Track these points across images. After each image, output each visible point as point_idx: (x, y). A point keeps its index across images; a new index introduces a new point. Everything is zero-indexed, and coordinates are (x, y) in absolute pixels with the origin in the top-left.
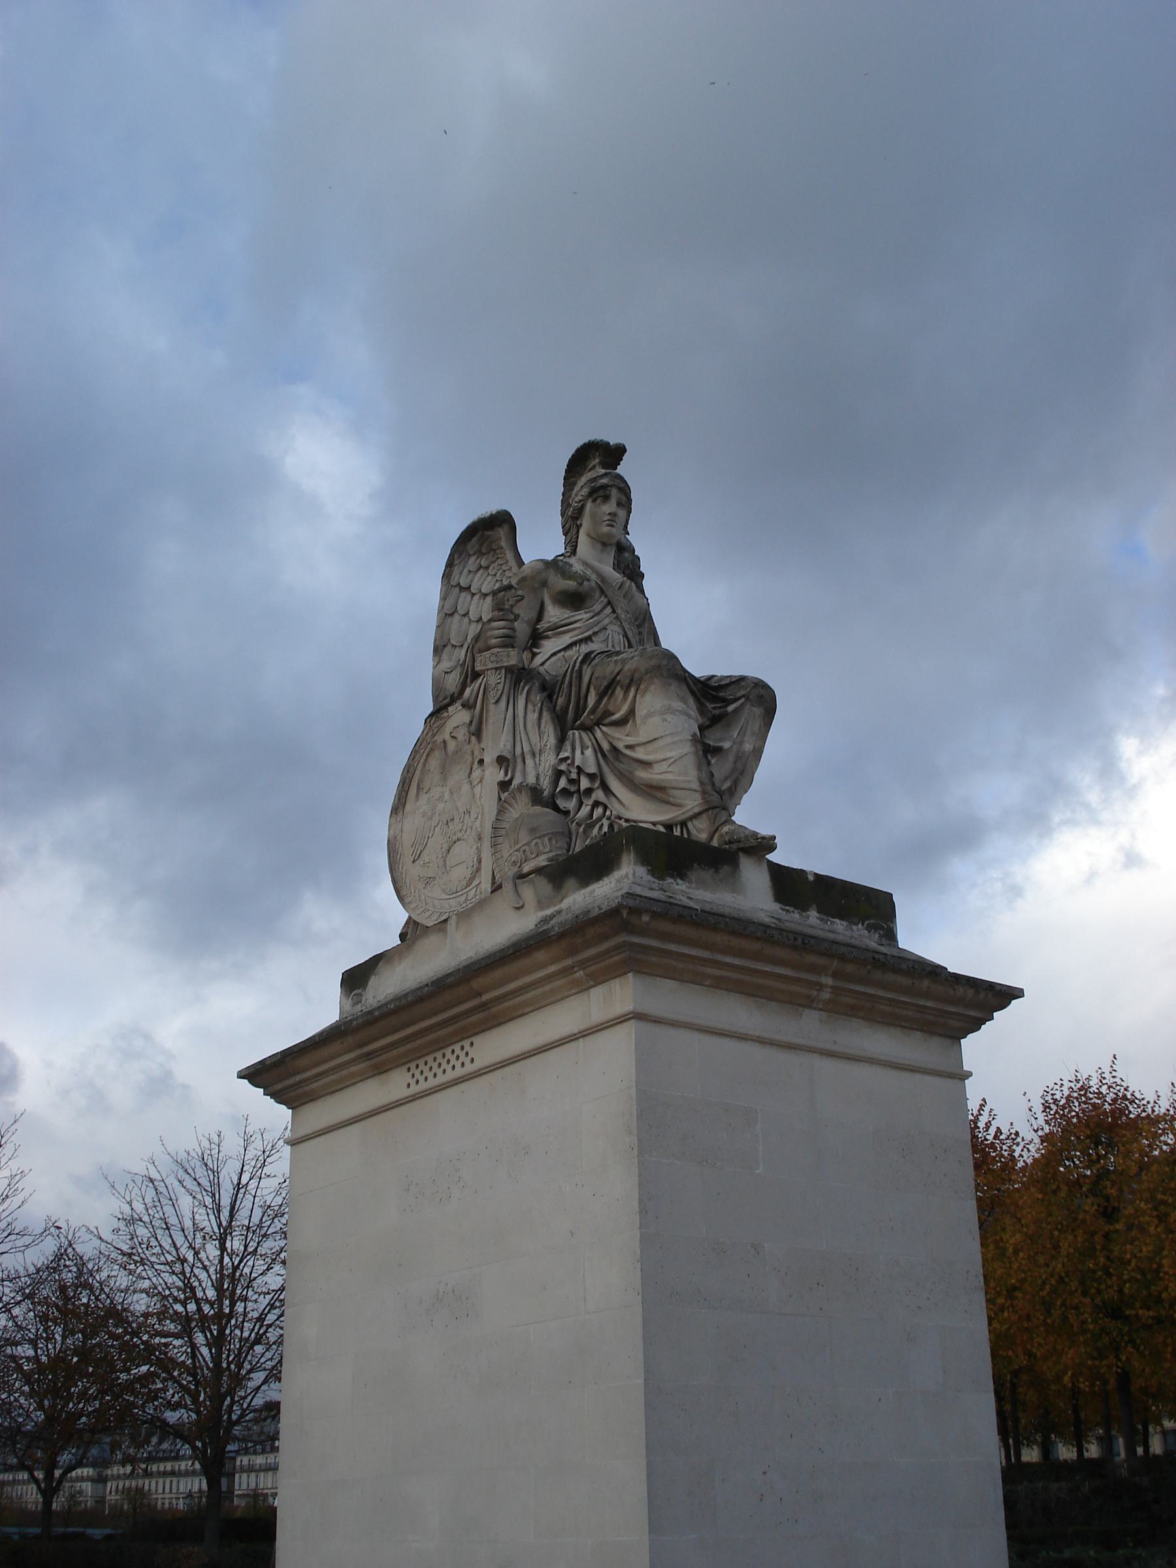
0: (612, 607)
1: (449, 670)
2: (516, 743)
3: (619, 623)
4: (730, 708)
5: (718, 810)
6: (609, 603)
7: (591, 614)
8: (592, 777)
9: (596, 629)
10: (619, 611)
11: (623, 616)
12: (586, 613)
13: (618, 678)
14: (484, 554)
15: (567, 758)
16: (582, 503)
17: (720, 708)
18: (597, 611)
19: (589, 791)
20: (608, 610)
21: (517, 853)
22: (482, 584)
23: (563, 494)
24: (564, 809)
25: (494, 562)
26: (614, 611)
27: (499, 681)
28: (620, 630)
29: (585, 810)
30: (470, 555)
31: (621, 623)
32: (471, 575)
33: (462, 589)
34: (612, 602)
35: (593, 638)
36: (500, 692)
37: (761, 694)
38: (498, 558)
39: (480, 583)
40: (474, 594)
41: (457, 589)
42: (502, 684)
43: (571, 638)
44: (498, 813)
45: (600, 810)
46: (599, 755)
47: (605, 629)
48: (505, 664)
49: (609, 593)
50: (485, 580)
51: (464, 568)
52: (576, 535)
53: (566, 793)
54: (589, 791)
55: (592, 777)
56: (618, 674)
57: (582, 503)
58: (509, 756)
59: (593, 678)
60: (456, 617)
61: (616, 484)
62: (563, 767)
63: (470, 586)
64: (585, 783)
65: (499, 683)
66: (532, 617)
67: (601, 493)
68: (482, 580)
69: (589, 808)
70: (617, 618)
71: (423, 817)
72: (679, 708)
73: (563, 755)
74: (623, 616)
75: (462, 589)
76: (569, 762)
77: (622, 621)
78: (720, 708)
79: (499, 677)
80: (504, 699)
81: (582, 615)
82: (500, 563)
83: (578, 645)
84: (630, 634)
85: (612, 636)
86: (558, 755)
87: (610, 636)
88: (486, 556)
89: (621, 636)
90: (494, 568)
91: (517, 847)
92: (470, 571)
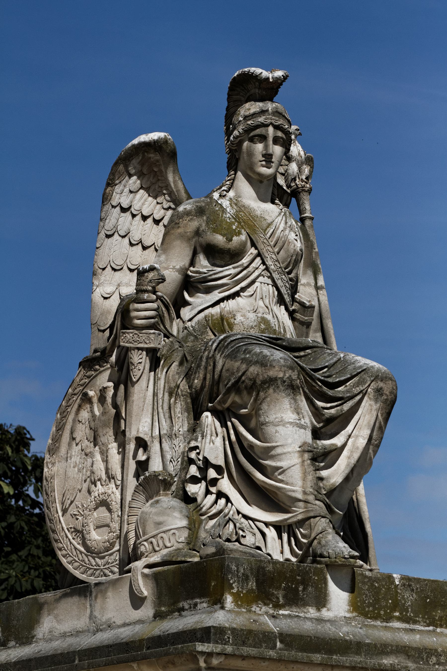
0: (262, 259)
1: (108, 296)
2: (154, 423)
3: (269, 275)
4: (346, 407)
5: (318, 518)
6: (259, 255)
7: (239, 269)
8: (218, 469)
9: (243, 284)
10: (269, 262)
11: (272, 267)
12: (234, 268)
13: (243, 378)
14: (146, 175)
15: (196, 448)
16: (239, 139)
17: (337, 406)
18: (245, 265)
19: (214, 482)
20: (258, 260)
21: (145, 543)
22: (143, 204)
23: (227, 109)
24: (192, 496)
25: (153, 184)
26: (264, 263)
27: (140, 361)
28: (269, 281)
29: (211, 498)
30: (130, 176)
31: (271, 274)
32: (132, 195)
33: (124, 210)
34: (261, 253)
35: (241, 294)
36: (141, 371)
37: (380, 387)
38: (159, 180)
39: (140, 204)
40: (134, 216)
41: (118, 209)
42: (143, 364)
43: (219, 293)
44: (134, 494)
45: (222, 501)
46: (227, 443)
47: (253, 282)
48: (146, 346)
49: (260, 246)
50: (145, 200)
51: (125, 186)
52: (235, 167)
53: (195, 480)
54: (214, 482)
55: (218, 469)
56: (243, 374)
57: (239, 139)
58: (147, 438)
59: (224, 370)
60: (116, 236)
61: (273, 121)
62: (193, 455)
63: (130, 207)
64: (212, 474)
65: (140, 363)
66: (184, 265)
67: (258, 131)
68: (142, 201)
69: (214, 496)
70: (267, 269)
71: (74, 467)
72: (290, 420)
73: (193, 444)
74: (272, 267)
75: (124, 210)
76: (198, 451)
77: (272, 272)
78: (337, 406)
79: (140, 357)
80: (145, 378)
81: (230, 270)
82: (160, 185)
83: (225, 301)
84: (279, 283)
85: (261, 289)
86: (189, 443)
87: (258, 290)
88: (147, 176)
89: (270, 286)
90: (155, 190)
91: (146, 537)
92: (131, 192)
